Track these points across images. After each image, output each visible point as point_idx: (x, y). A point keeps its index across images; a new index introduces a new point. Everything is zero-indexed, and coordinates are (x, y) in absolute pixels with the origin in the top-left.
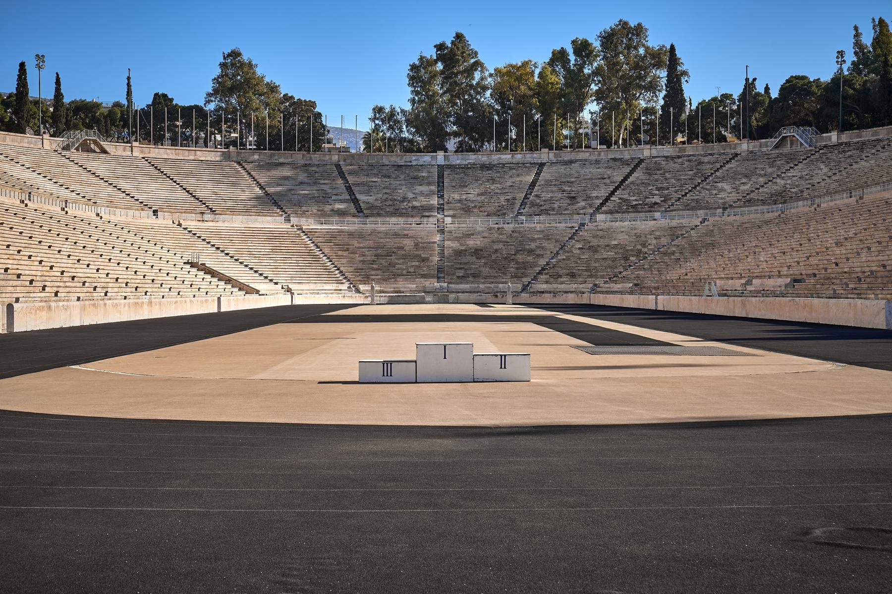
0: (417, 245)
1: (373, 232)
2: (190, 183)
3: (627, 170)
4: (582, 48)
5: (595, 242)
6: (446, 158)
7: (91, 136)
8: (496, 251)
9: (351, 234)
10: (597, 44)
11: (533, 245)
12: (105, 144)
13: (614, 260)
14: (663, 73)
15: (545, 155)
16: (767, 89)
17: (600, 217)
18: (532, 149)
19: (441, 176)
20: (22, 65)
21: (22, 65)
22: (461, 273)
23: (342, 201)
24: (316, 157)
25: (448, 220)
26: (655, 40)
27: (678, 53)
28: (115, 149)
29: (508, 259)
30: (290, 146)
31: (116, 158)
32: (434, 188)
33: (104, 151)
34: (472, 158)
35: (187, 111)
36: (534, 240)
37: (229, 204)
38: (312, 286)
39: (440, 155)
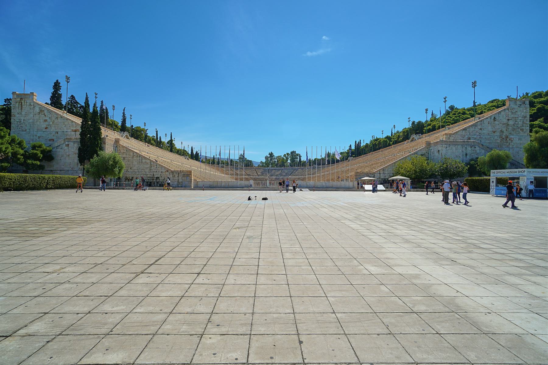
1: (260, 178)
3: (293, 170)
4: (288, 154)
10: (290, 153)
14: (298, 157)
15: (283, 168)
16: (312, 160)
17: (290, 176)
18: (281, 167)
19: (269, 171)
20: (214, 156)
21: (214, 156)
26: (297, 153)
27: (301, 155)
34: (273, 168)
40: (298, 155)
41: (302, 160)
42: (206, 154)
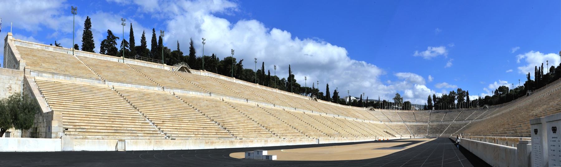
0: (425, 127)
2: (388, 116)
5: (453, 126)
6: (431, 111)
7: (372, 107)
8: (438, 128)
9: (414, 125)
11: (443, 127)
12: (374, 109)
13: (456, 130)
15: (447, 110)
18: (445, 109)
19: (430, 115)
20: (361, 95)
21: (361, 95)
22: (431, 132)
23: (413, 119)
24: (410, 111)
25: (430, 122)
28: (376, 110)
29: (439, 130)
30: (406, 109)
31: (376, 112)
32: (429, 116)
33: (374, 110)
35: (388, 103)
36: (444, 126)
37: (394, 120)
38: (406, 135)
39: (430, 110)
40: (464, 92)
41: (470, 100)
42: (348, 93)
